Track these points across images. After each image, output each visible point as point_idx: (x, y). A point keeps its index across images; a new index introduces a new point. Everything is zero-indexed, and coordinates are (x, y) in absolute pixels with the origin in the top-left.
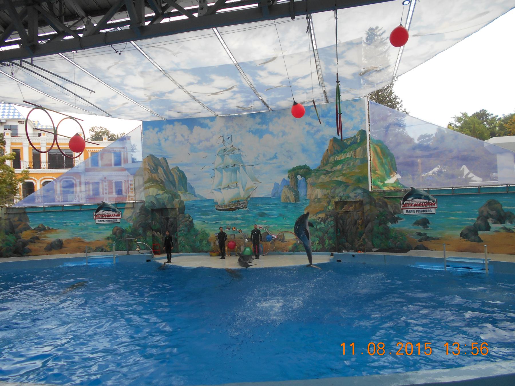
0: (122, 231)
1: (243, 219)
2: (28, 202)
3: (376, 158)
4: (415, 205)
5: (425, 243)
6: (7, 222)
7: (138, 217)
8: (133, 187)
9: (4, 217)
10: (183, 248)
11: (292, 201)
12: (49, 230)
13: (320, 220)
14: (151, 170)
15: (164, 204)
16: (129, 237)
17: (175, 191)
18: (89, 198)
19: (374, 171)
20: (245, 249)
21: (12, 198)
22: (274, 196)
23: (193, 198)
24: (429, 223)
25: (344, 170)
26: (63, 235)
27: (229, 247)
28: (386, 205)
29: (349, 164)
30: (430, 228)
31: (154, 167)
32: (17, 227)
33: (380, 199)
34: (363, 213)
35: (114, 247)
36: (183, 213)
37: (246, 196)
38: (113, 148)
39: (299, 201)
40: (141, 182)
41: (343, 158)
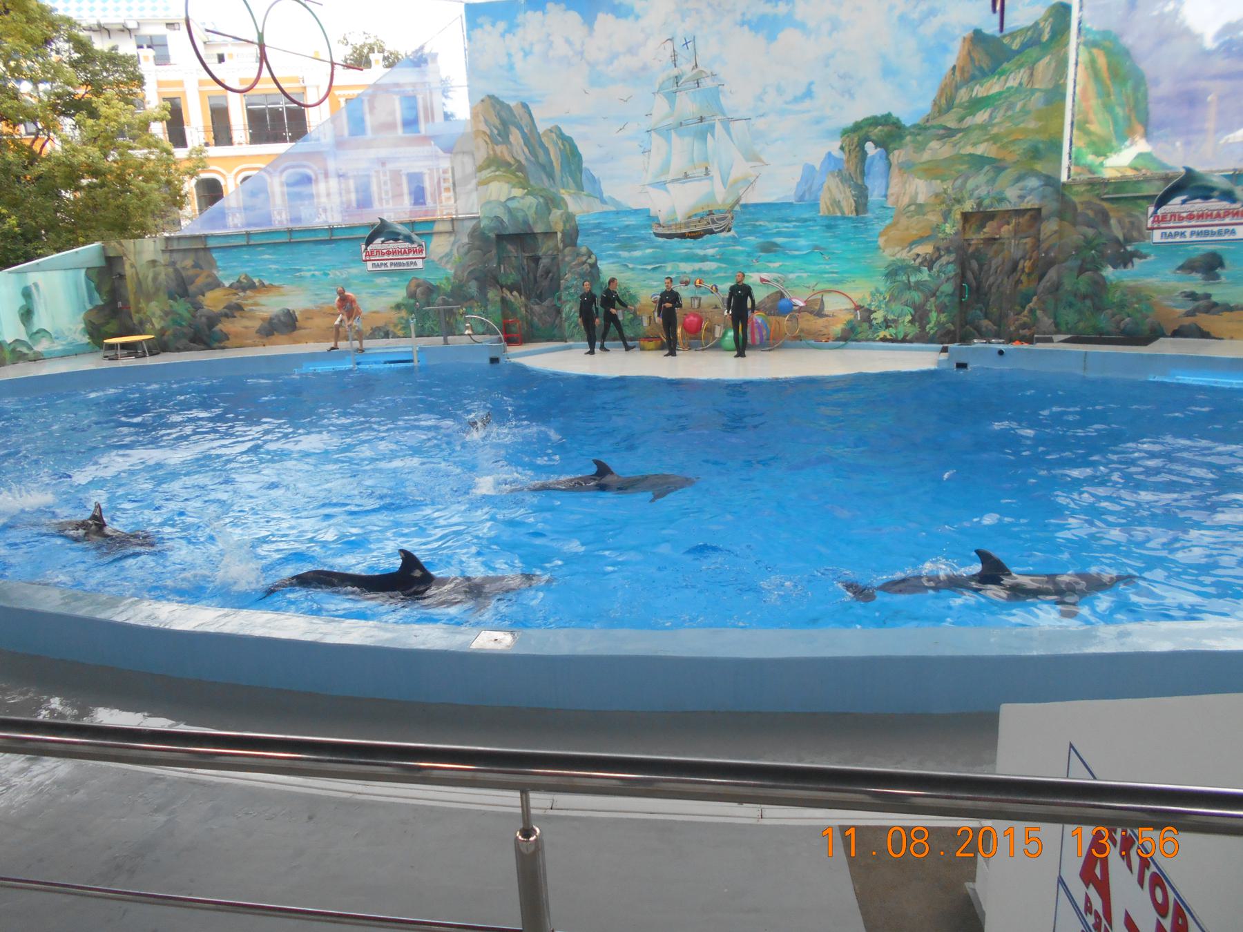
0: (430, 290)
1: (722, 258)
2: (212, 221)
3: (1092, 88)
4: (1191, 217)
5: (1204, 321)
6: (171, 270)
7: (466, 254)
8: (450, 184)
9: (162, 259)
10: (575, 331)
11: (846, 210)
12: (263, 288)
13: (919, 260)
14: (491, 137)
15: (526, 222)
16: (445, 303)
17: (553, 190)
18: (346, 209)
19: (1080, 125)
20: (724, 335)
21: (174, 216)
22: (801, 199)
23: (598, 207)
24: (1221, 265)
25: (994, 125)
26: (297, 301)
27: (685, 327)
28: (1105, 217)
29: (1011, 107)
30: (1223, 279)
31: (500, 127)
32: (193, 282)
33: (1088, 204)
34: (1037, 243)
35: (412, 326)
36: (574, 244)
37: (730, 200)
38: (397, 85)
39: (866, 211)
40: (470, 168)
41: (996, 89)
